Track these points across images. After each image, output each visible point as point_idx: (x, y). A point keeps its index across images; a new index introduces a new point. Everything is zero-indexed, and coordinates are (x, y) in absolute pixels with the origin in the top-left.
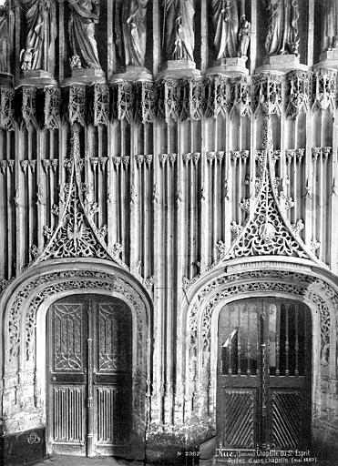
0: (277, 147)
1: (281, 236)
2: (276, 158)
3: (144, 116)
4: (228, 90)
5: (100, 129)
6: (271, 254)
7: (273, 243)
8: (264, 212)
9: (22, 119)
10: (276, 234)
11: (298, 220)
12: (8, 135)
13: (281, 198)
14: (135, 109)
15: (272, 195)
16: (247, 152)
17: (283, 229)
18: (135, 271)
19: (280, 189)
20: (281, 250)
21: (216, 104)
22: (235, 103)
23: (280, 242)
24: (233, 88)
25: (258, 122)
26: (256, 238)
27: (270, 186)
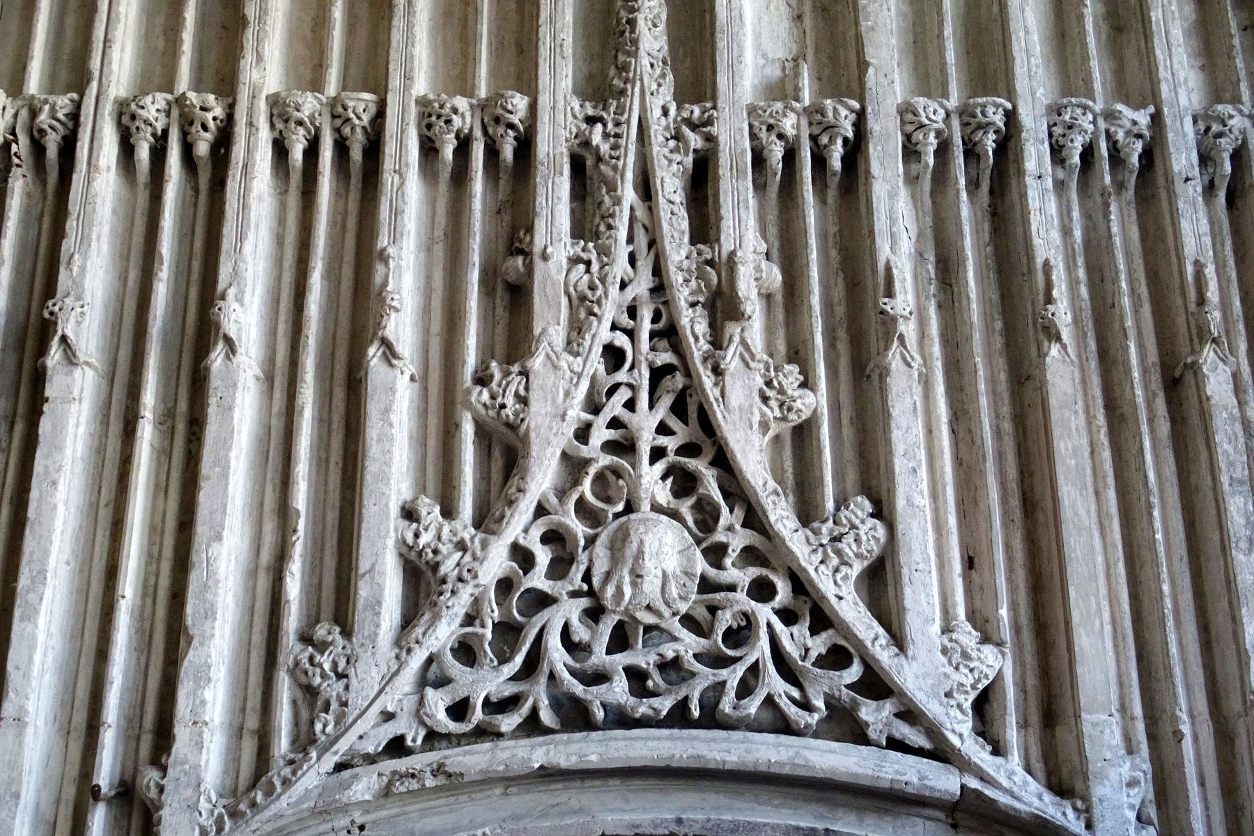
1: (742, 600)
2: (695, 140)
6: (679, 717)
7: (688, 644)
8: (624, 447)
10: (706, 585)
11: (842, 502)
13: (731, 359)
15: (677, 347)
16: (519, 103)
17: (750, 555)
20: (745, 690)
23: (740, 635)
26: (571, 611)
27: (660, 288)
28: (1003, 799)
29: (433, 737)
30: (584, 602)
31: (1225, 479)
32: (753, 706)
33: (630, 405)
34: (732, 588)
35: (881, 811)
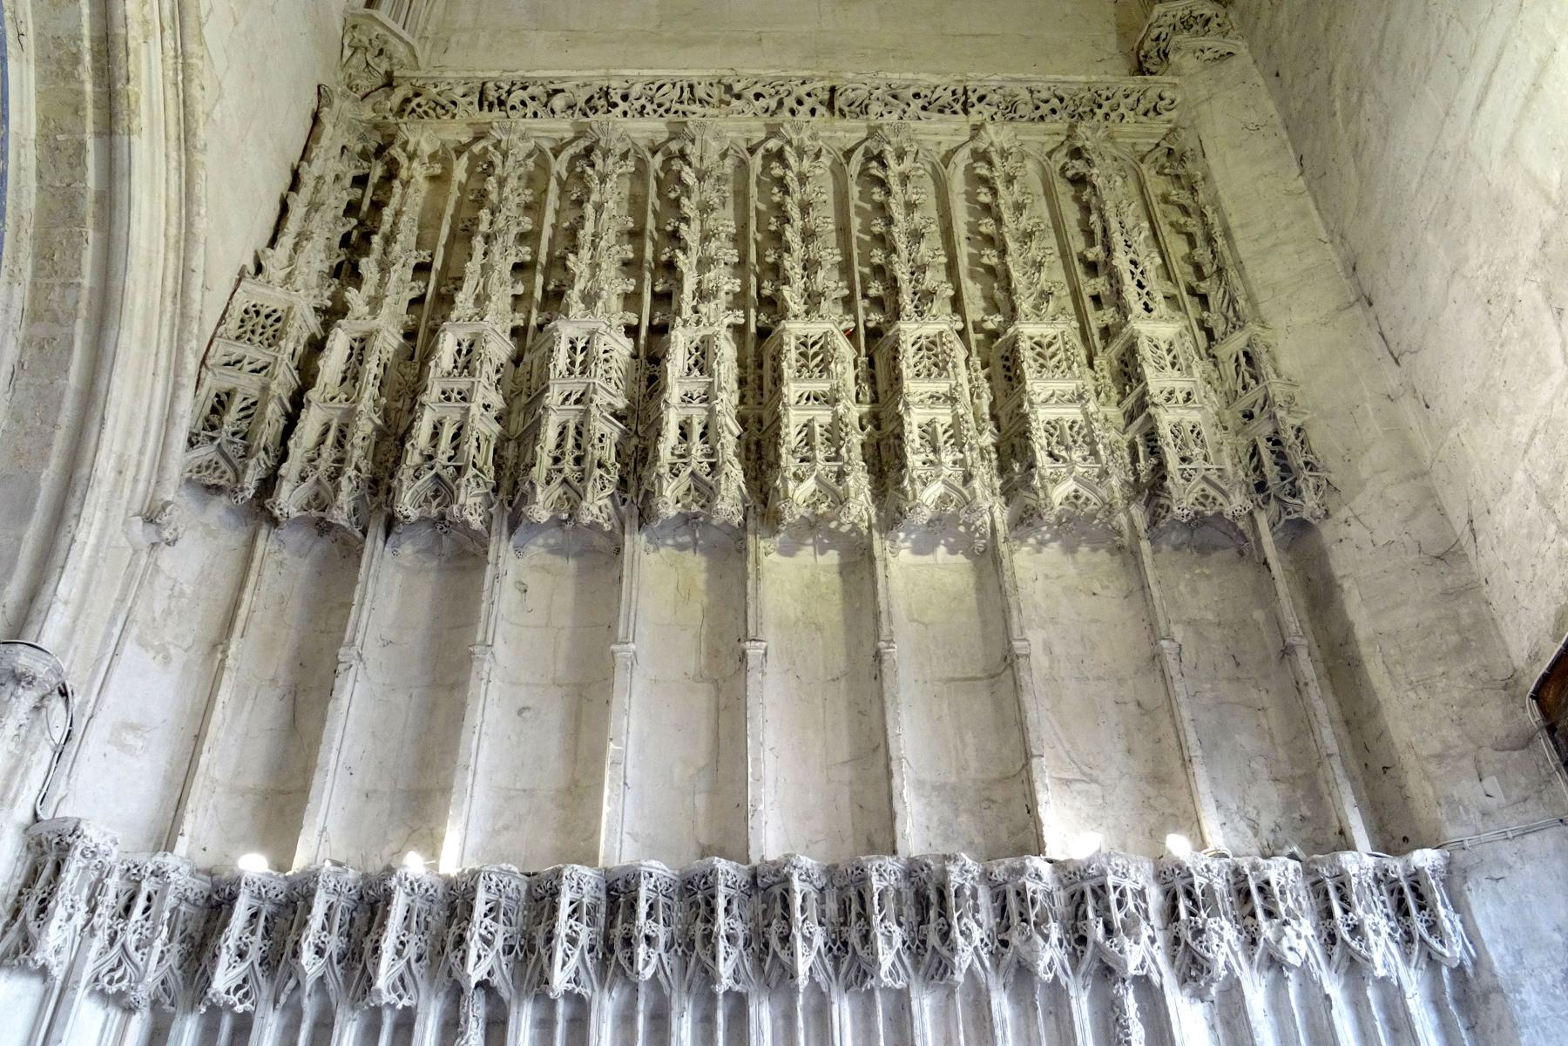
3: (725, 969)
4: (984, 898)
5: (561, 1009)
9: (294, 972)
12: (226, 1023)
14: (691, 945)
21: (961, 940)
22: (1015, 939)
24: (1000, 898)
25: (1091, 999)
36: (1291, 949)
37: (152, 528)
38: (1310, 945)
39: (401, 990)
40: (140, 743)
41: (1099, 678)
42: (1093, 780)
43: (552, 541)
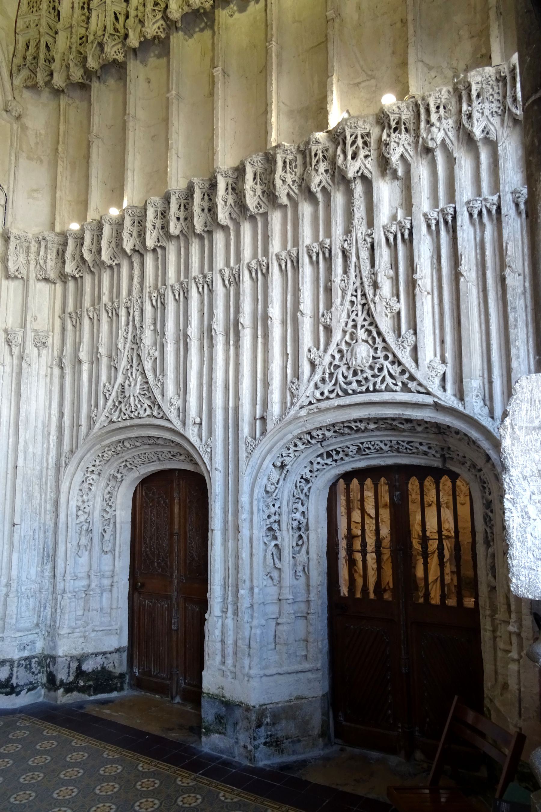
0: (370, 224)
1: (382, 360)
6: (367, 390)
10: (374, 358)
16: (328, 241)
18: (192, 434)
19: (375, 286)
23: (381, 370)
26: (343, 368)
27: (362, 283)
28: (442, 403)
29: (319, 401)
30: (346, 366)
31: (509, 308)
32: (383, 387)
33: (357, 315)
34: (379, 358)
35: (419, 408)
36: (432, 139)
37: (8, 113)
38: (446, 133)
39: (113, 259)
40: (40, 196)
41: (384, 14)
42: (372, 77)
43: (157, 52)
